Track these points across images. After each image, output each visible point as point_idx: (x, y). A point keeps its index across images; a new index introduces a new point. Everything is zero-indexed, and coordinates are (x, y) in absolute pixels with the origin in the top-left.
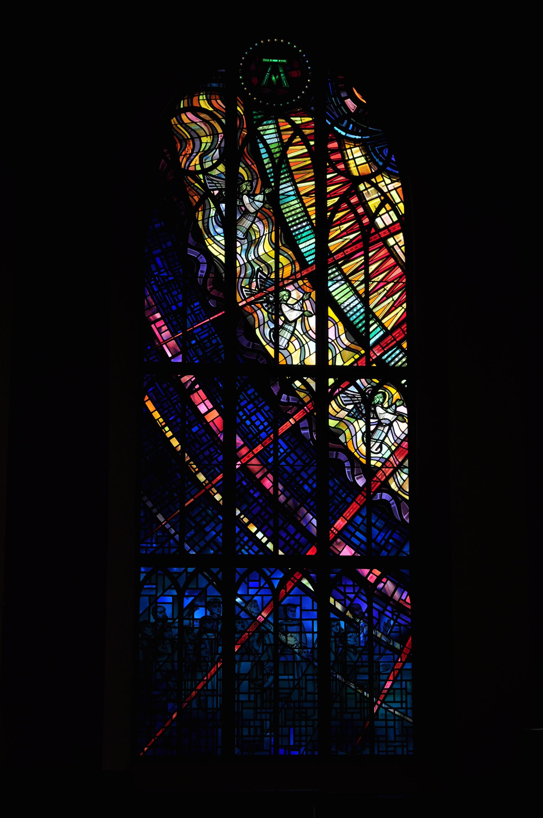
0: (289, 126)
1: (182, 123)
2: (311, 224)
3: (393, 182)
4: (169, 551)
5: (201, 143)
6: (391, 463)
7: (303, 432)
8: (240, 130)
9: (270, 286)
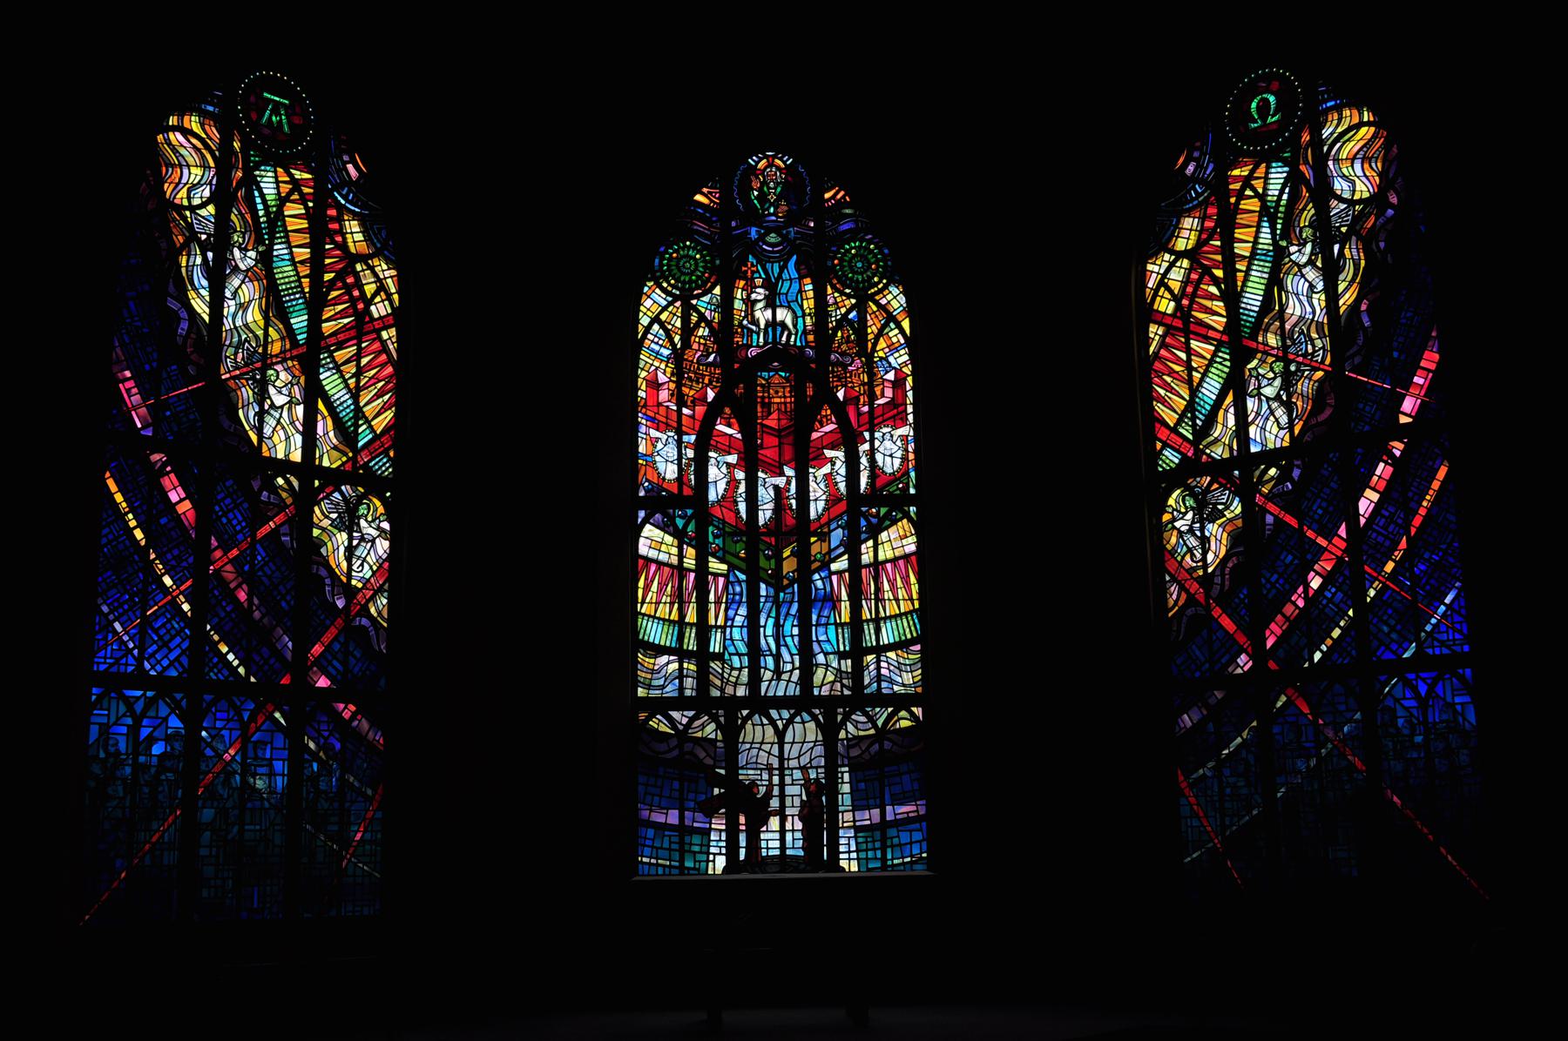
0: (288, 179)
1: (169, 143)
2: (304, 297)
3: (389, 269)
4: (126, 670)
5: (190, 173)
6: (372, 584)
7: (283, 539)
8: (234, 170)
9: (258, 362)
